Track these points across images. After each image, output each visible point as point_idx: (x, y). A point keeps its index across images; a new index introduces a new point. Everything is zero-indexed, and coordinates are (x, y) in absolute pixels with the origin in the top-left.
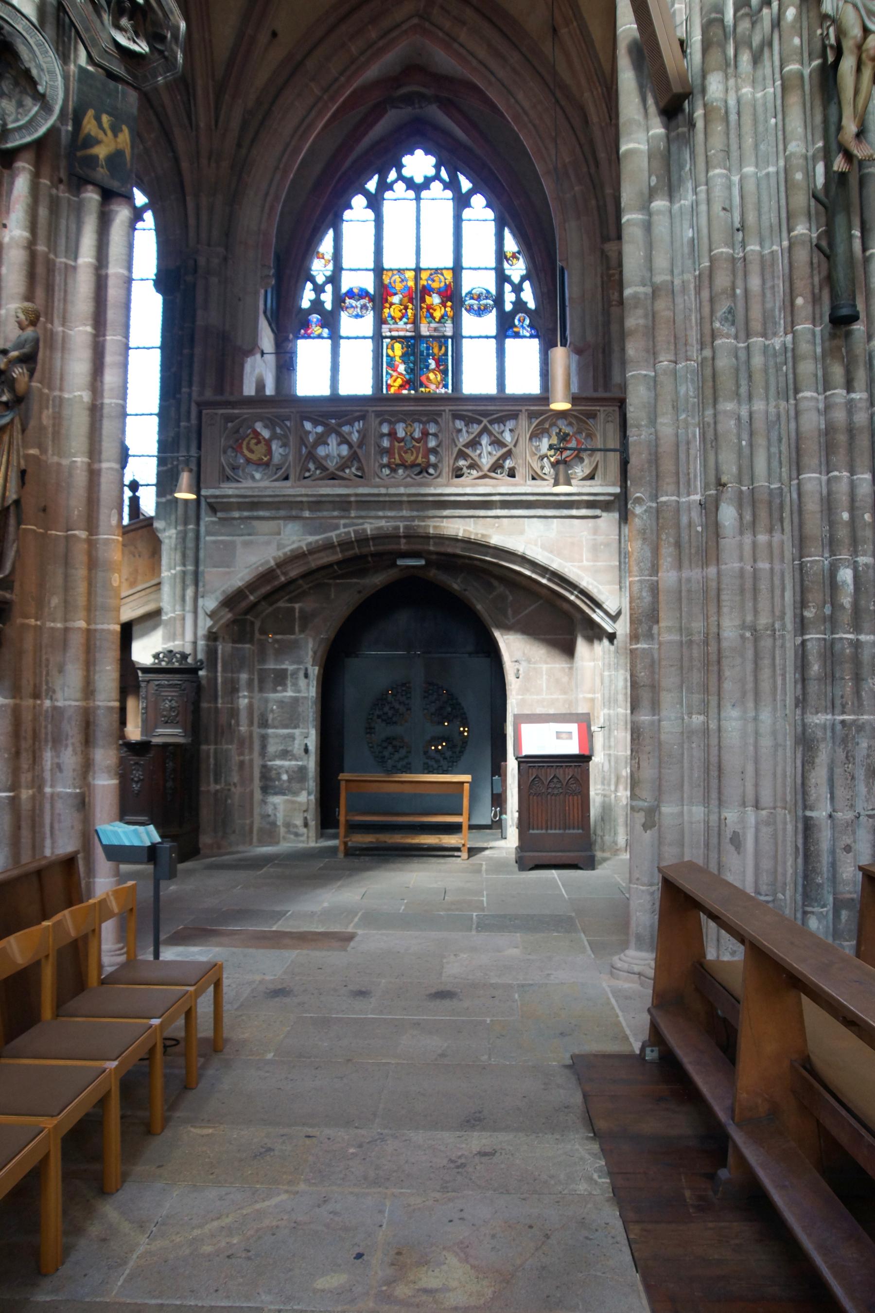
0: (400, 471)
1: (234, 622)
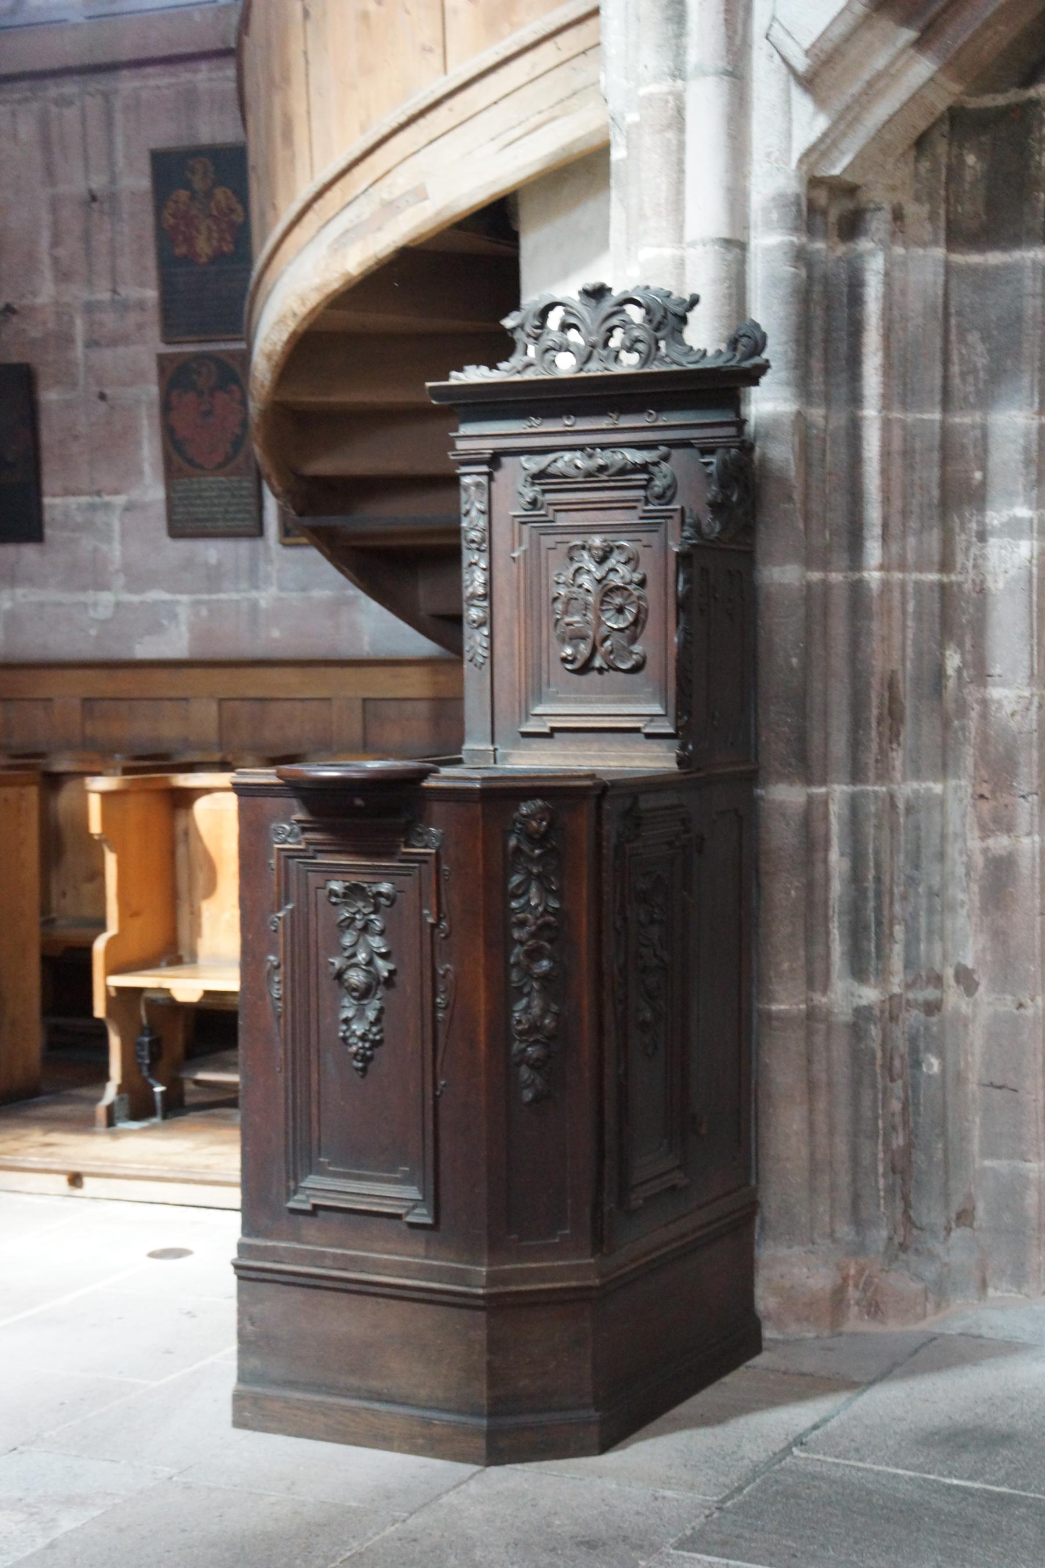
1: (958, 122)
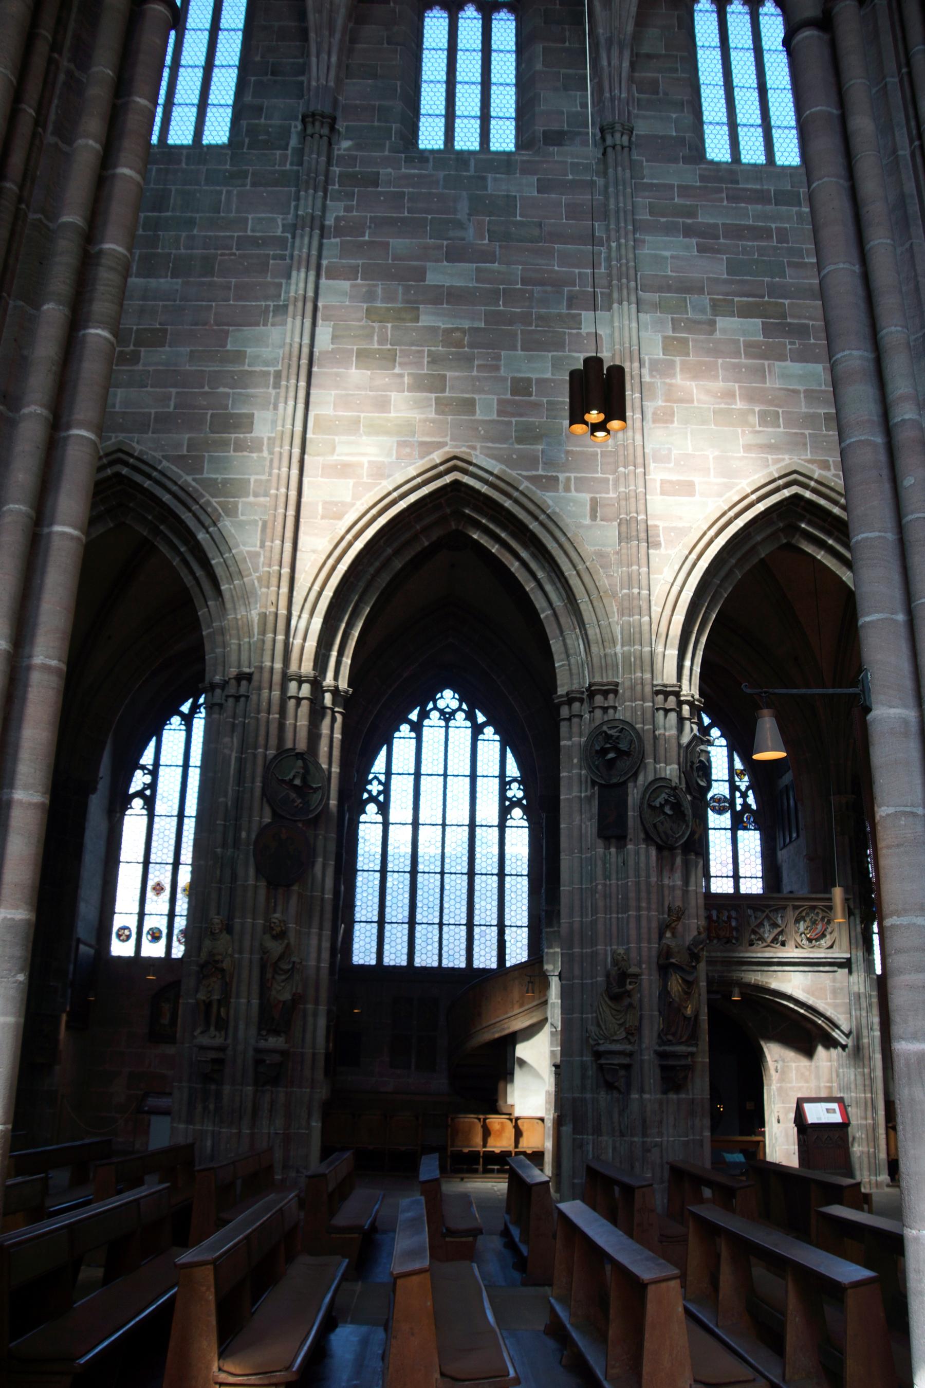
0: (715, 941)
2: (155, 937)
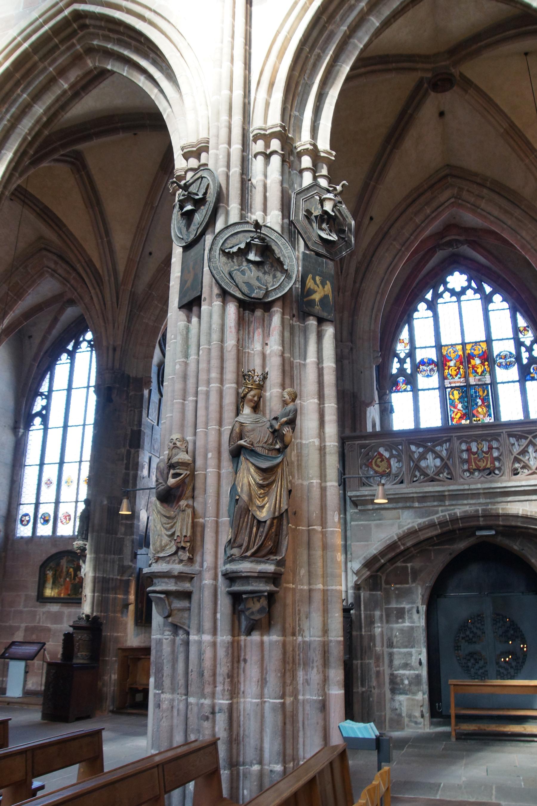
0: (476, 474)
1: (370, 577)
2: (46, 522)
